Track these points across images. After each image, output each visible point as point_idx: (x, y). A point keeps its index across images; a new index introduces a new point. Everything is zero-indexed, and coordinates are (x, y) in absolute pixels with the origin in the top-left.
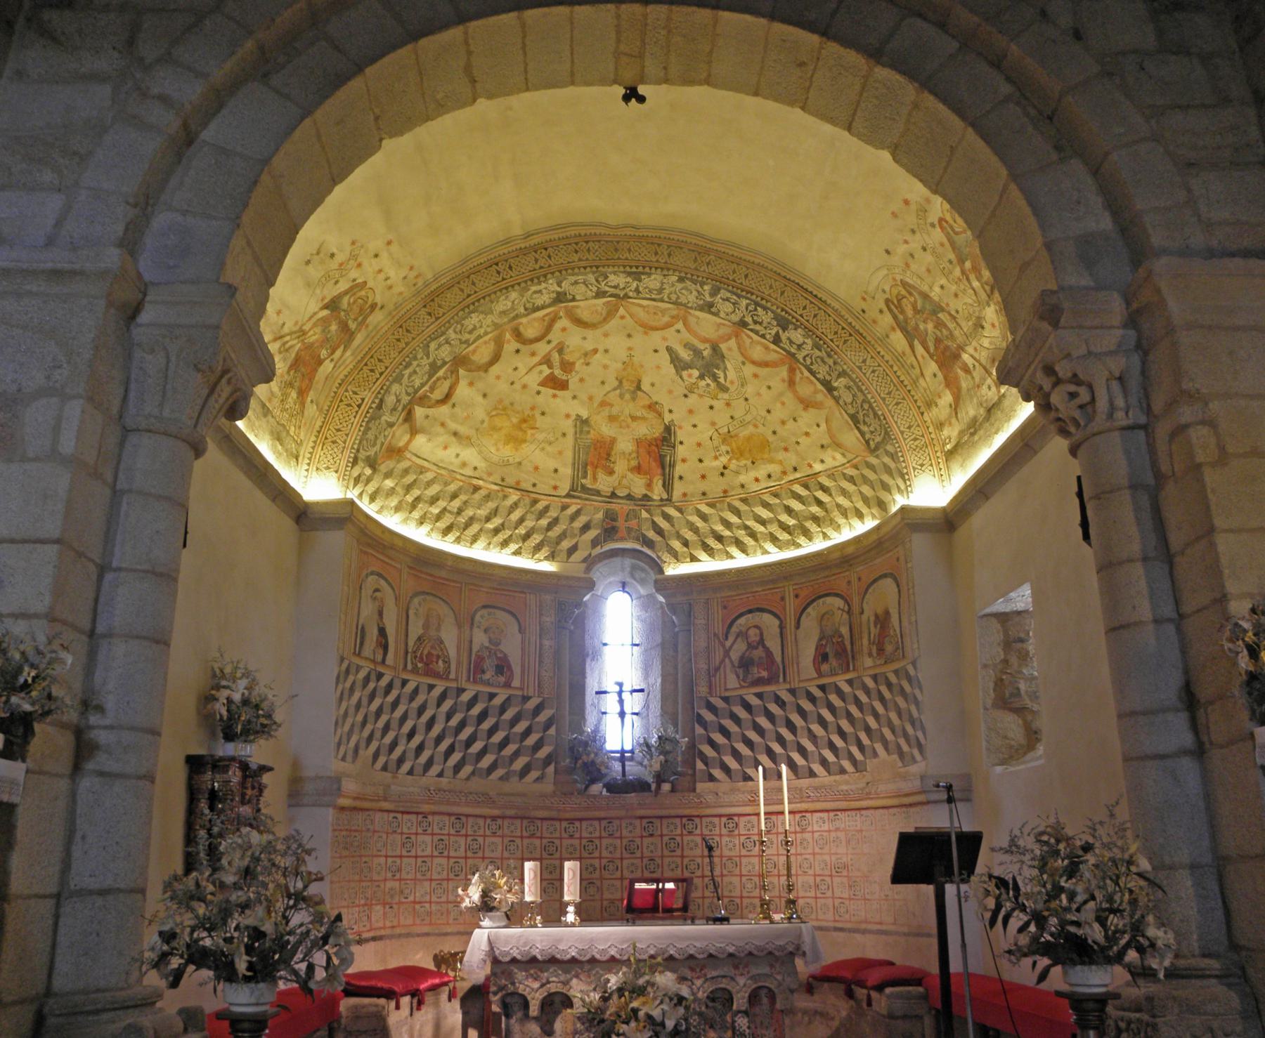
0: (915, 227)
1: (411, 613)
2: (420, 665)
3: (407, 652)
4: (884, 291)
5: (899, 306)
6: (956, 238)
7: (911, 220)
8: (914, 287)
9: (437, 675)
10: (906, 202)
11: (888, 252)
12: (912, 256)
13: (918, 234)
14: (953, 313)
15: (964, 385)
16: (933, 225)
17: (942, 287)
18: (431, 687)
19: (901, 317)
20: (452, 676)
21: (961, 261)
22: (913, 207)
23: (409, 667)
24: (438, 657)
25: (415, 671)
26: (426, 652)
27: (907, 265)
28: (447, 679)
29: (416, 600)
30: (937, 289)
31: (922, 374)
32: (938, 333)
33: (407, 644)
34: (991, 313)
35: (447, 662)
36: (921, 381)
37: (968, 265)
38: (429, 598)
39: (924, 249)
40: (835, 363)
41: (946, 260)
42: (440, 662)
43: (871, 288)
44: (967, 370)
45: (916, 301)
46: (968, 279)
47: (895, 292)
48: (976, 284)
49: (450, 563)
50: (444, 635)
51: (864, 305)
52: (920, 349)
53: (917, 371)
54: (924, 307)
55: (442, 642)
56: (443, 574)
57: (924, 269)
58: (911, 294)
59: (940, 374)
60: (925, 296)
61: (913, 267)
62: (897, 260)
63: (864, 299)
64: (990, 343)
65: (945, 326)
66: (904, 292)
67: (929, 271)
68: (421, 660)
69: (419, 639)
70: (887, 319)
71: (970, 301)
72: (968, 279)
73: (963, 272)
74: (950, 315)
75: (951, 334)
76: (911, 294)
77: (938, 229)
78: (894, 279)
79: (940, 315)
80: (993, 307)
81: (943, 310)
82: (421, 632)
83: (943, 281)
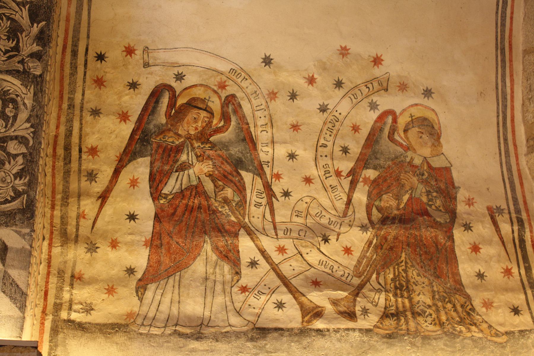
0: (348, 85)
4: (179, 77)
5: (177, 114)
6: (385, 142)
7: (354, 76)
8: (242, 118)
10: (377, 61)
11: (267, 61)
12: (293, 96)
13: (340, 93)
14: (277, 189)
15: (199, 267)
16: (373, 106)
17: (292, 156)
19: (161, 118)
21: (363, 162)
22: (378, 72)
27: (273, 95)
30: (281, 151)
31: (104, 197)
32: (209, 186)
34: (357, 238)
36: (89, 206)
37: (371, 174)
39: (323, 109)
40: (37, 56)
41: (340, 142)
43: (162, 56)
44: (231, 256)
45: (218, 131)
46: (353, 184)
47: (199, 93)
48: (361, 196)
51: (115, 54)
52: (141, 169)
53: (98, 187)
54: (225, 146)
57: (291, 120)
58: (225, 117)
59: (147, 226)
60: (249, 140)
61: (280, 106)
62: (266, 79)
63: (130, 51)
64: (321, 263)
65: (241, 189)
66: (216, 105)
67: (295, 127)
70: (136, 103)
71: (325, 202)
72: (353, 184)
73: (353, 173)
74: (268, 187)
75: (243, 203)
76: (225, 117)
77: (374, 115)
78: (223, 86)
79: (247, 177)
80: (368, 235)
81: (259, 170)
83: (305, 154)
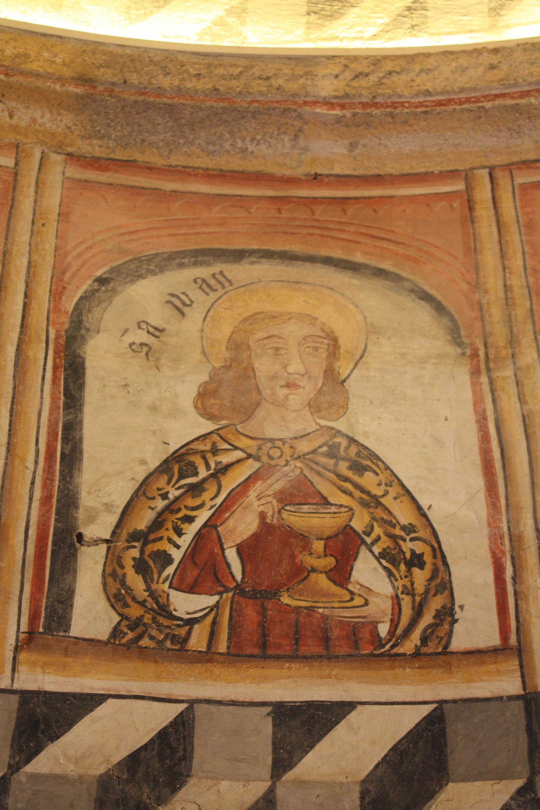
1: (101, 354)
2: (185, 604)
3: (63, 543)
9: (360, 647)
18: (301, 726)
20: (476, 625)
23: (91, 613)
24: (344, 547)
25: (146, 634)
26: (242, 525)
28: (436, 652)
29: (146, 295)
33: (67, 502)
35: (418, 556)
38: (240, 272)
42: (367, 571)
49: (326, 87)
50: (370, 423)
55: (365, 460)
56: (330, 152)
68: (203, 568)
69: (178, 462)
82: (187, 427)
